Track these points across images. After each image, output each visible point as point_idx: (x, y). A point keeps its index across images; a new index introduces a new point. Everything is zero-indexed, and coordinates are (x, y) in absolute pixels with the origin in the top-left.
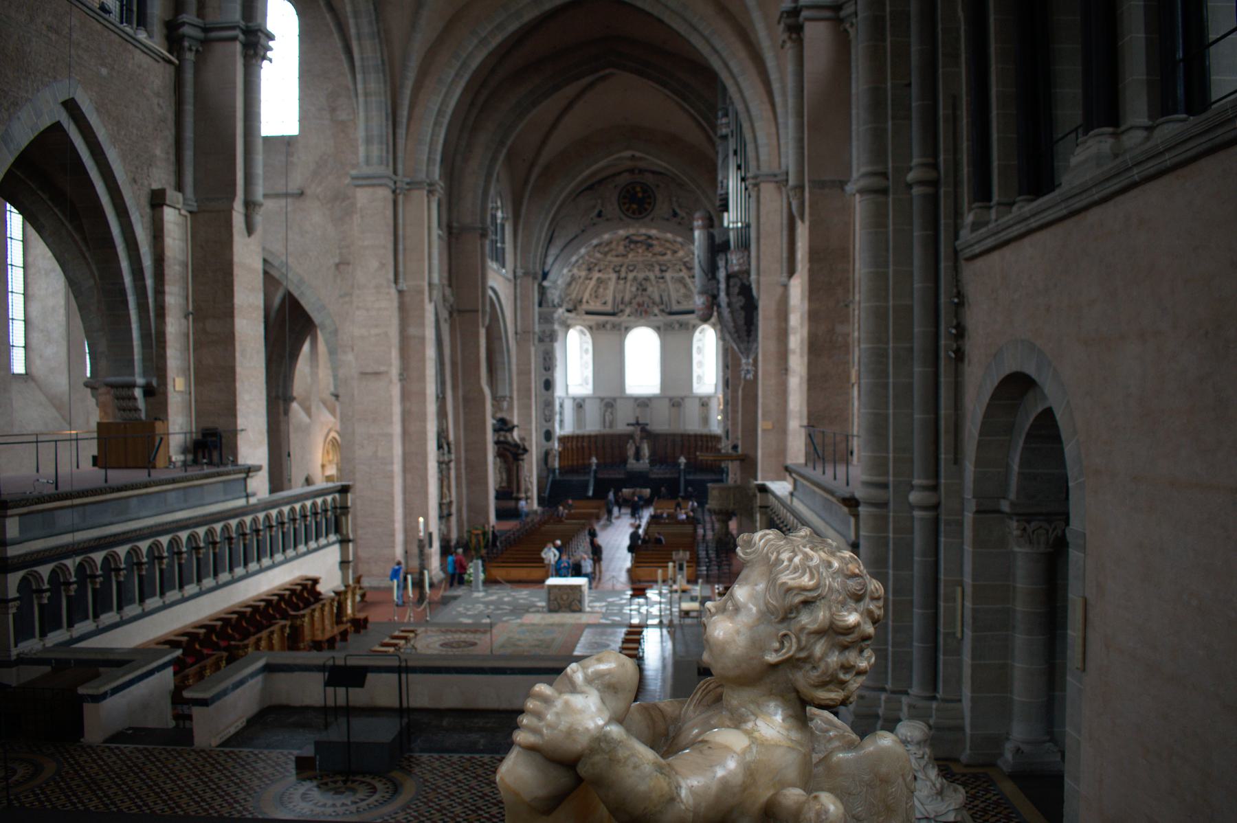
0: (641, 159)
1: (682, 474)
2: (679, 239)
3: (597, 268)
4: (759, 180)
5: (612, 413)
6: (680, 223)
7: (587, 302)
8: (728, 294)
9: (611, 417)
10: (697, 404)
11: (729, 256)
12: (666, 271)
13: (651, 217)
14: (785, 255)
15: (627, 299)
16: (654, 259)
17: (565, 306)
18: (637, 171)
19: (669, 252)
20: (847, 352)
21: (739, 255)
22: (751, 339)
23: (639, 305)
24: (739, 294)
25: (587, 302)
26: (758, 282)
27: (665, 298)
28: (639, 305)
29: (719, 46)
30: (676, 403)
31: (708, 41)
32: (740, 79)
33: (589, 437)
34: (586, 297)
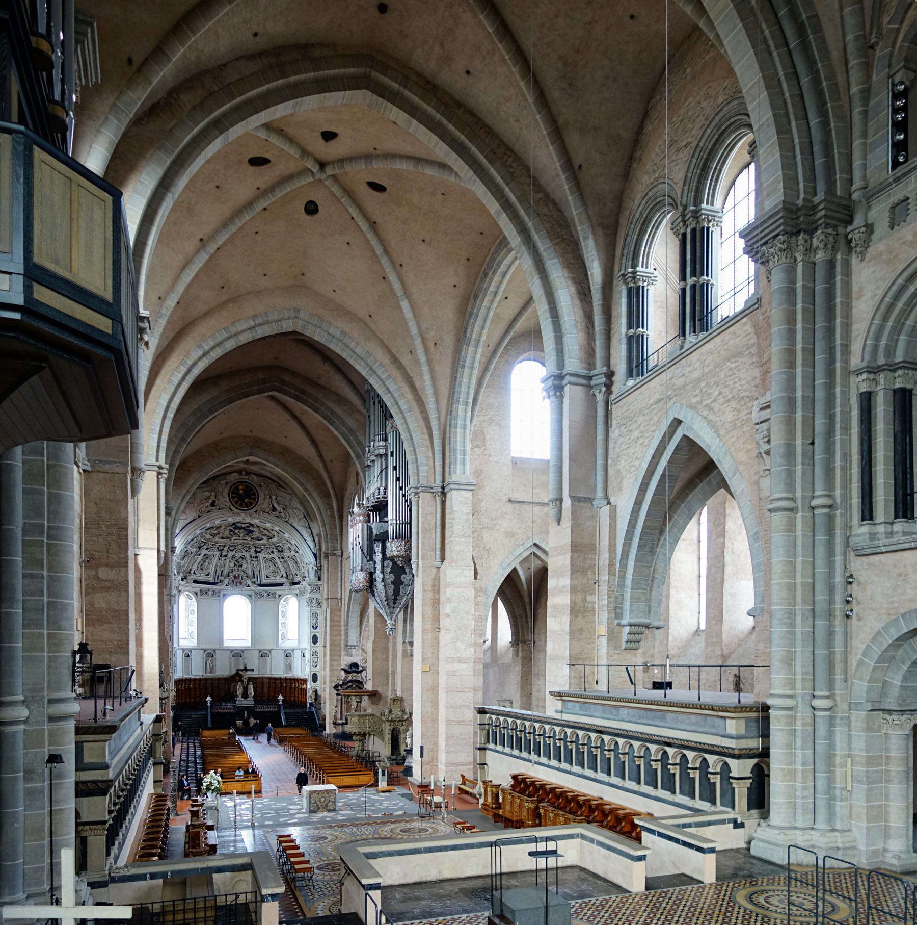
0: (255, 463)
2: (277, 529)
3: (205, 547)
8: (383, 572)
11: (388, 544)
13: (254, 509)
15: (225, 572)
17: (181, 575)
19: (265, 538)
20: (594, 615)
21: (398, 544)
23: (235, 577)
27: (257, 573)
28: (235, 577)
29: (392, 387)
31: (384, 383)
34: (194, 568)
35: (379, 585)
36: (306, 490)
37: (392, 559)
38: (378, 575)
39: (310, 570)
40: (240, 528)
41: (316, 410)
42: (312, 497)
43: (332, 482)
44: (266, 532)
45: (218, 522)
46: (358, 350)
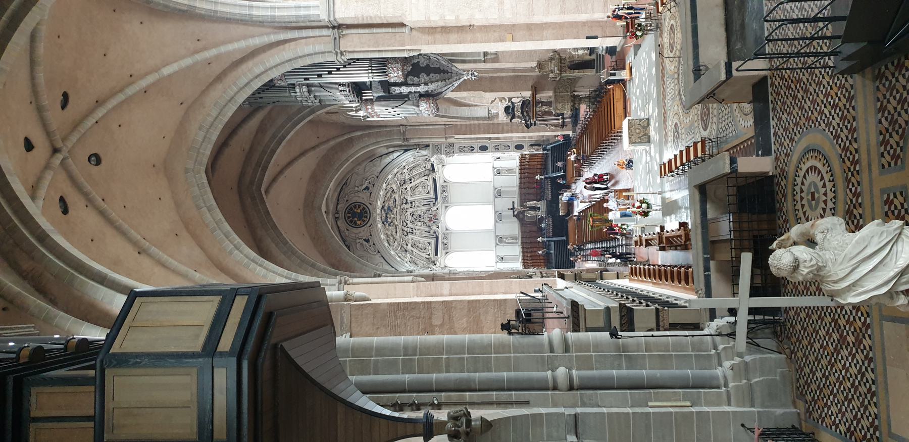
0: (327, 206)
1: (547, 176)
2: (384, 185)
3: (405, 246)
4: (339, 51)
5: (507, 238)
6: (373, 185)
7: (429, 255)
8: (419, 85)
9: (509, 239)
10: (498, 178)
11: (392, 80)
12: (407, 200)
13: (369, 205)
14: (390, 30)
15: (427, 229)
16: (399, 208)
17: (431, 266)
18: (337, 215)
21: (391, 71)
22: (449, 71)
23: (430, 221)
24: (419, 78)
25: (429, 255)
26: (409, 50)
28: (430, 221)
29: (245, 80)
30: (499, 194)
31: (241, 89)
32: (268, 65)
33: (523, 252)
34: (425, 255)
35: (431, 87)
36: (347, 160)
37: (406, 76)
38: (422, 89)
39: (420, 154)
40: (387, 217)
41: (273, 152)
42: (354, 155)
43: (338, 136)
44: (388, 195)
45: (382, 236)
46: (214, 113)
